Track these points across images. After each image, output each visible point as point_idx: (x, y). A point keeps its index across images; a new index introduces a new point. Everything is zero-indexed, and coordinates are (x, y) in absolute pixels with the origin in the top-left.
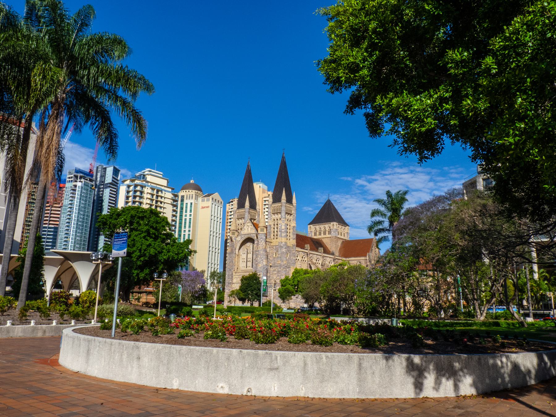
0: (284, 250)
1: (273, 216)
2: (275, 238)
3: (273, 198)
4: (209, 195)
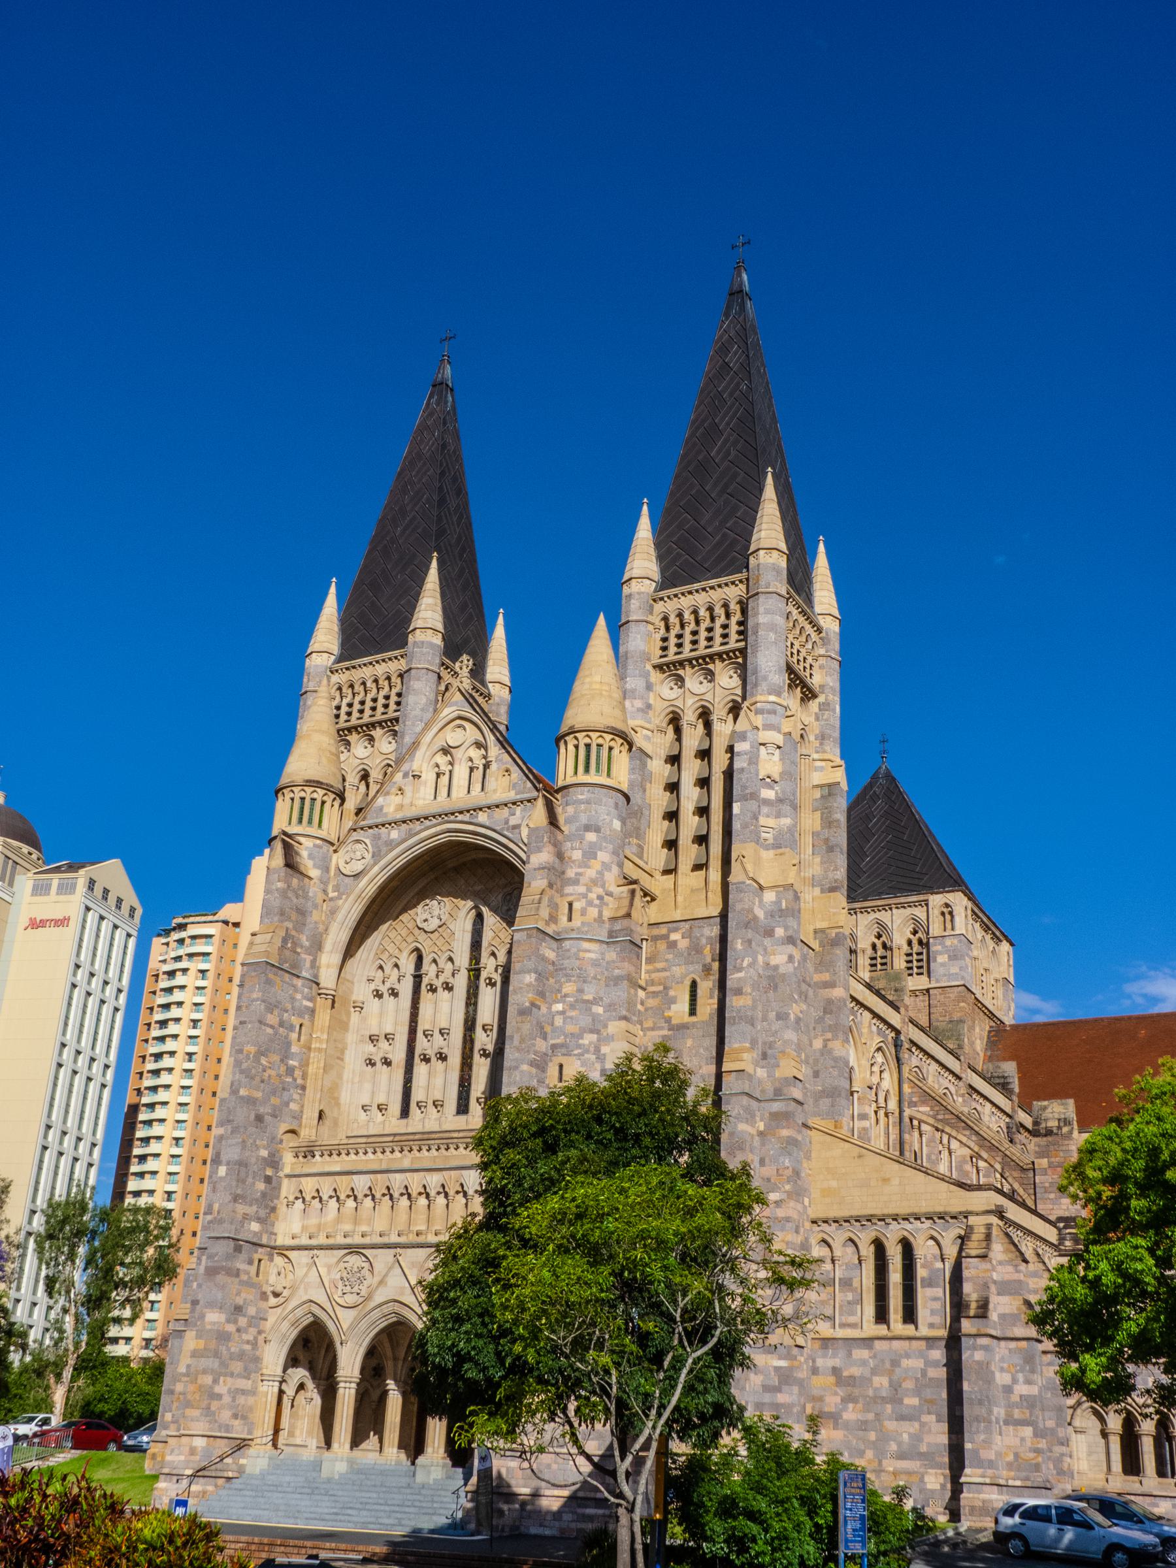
0: (779, 959)
1: (666, 690)
2: (686, 863)
3: (660, 558)
4: (73, 867)
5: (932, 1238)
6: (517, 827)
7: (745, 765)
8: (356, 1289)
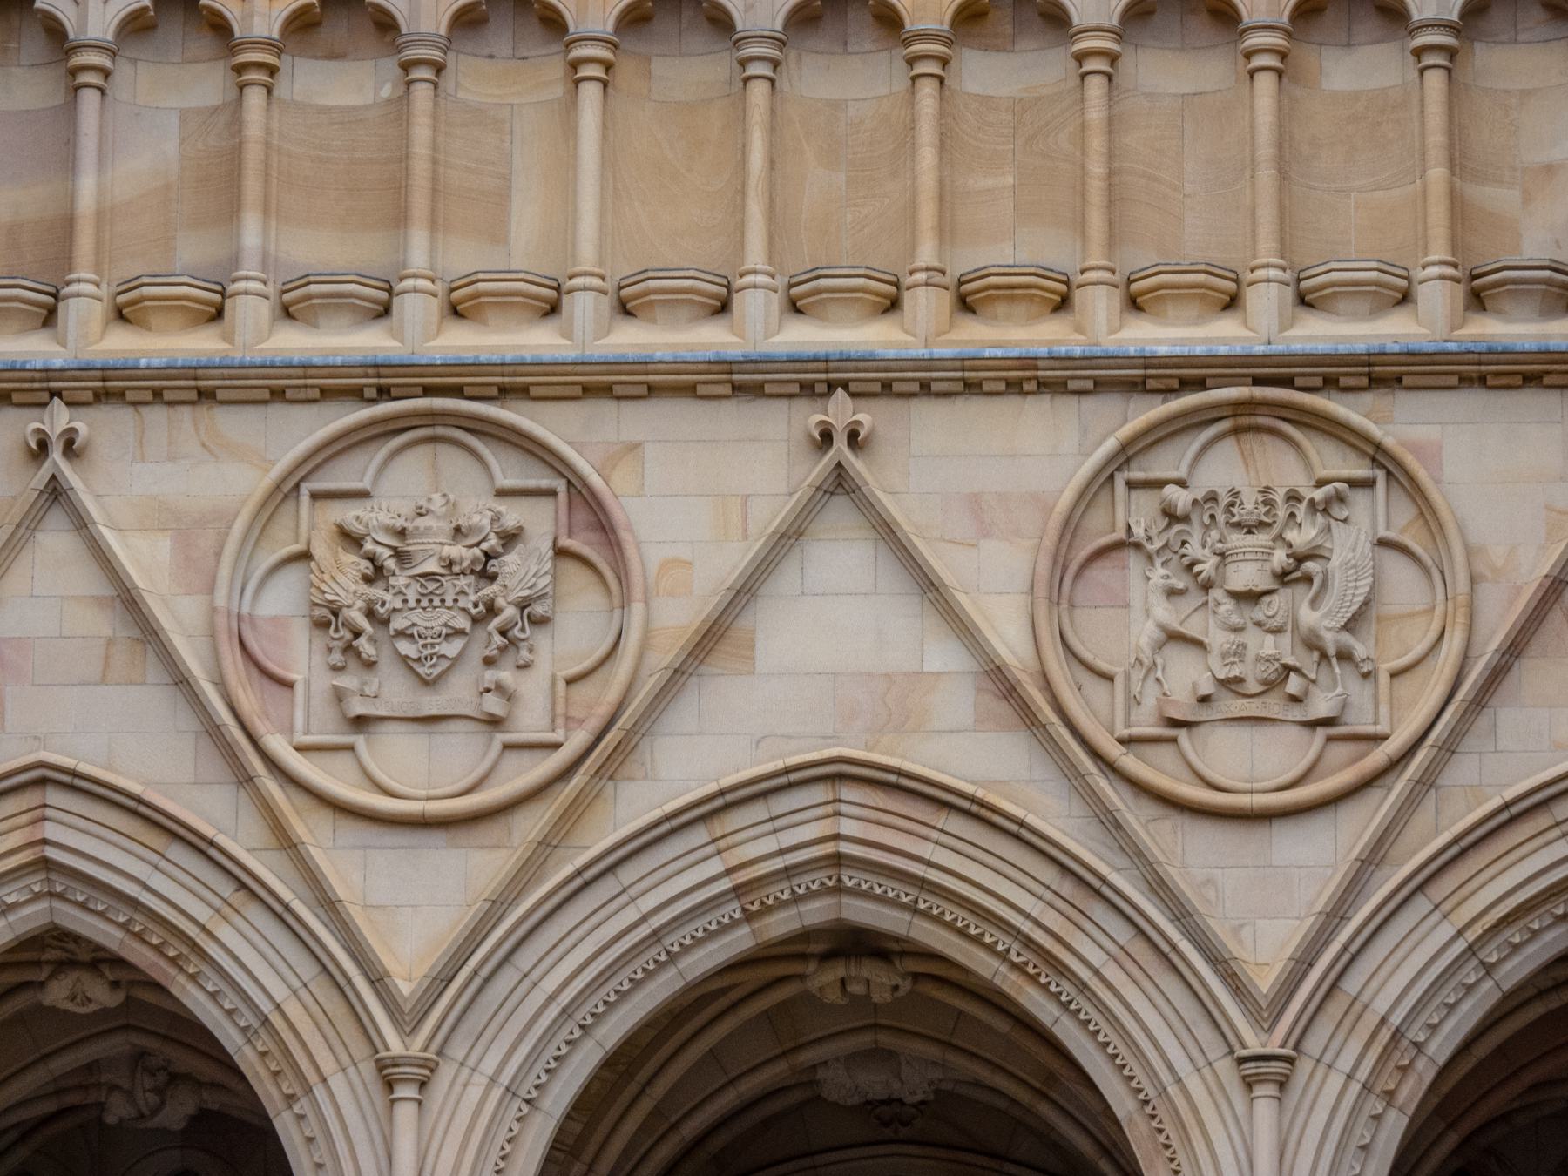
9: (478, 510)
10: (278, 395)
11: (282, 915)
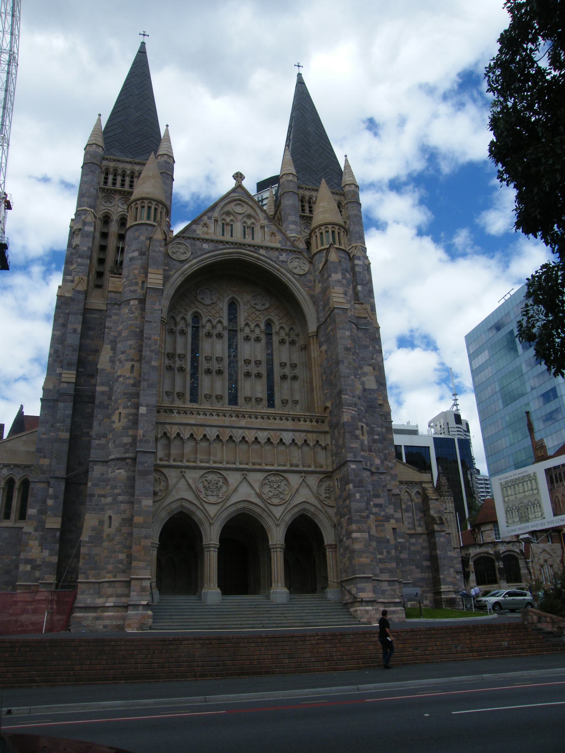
5: (407, 492)
6: (286, 262)
7: (361, 270)
8: (215, 493)
9: (216, 479)
10: (201, 469)
11: (202, 511)
